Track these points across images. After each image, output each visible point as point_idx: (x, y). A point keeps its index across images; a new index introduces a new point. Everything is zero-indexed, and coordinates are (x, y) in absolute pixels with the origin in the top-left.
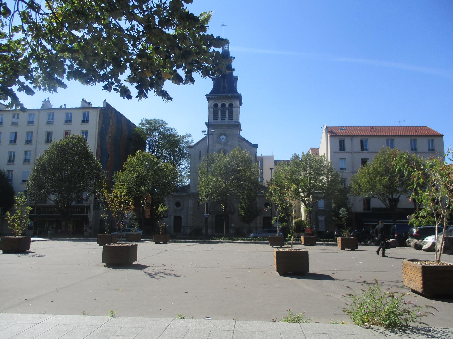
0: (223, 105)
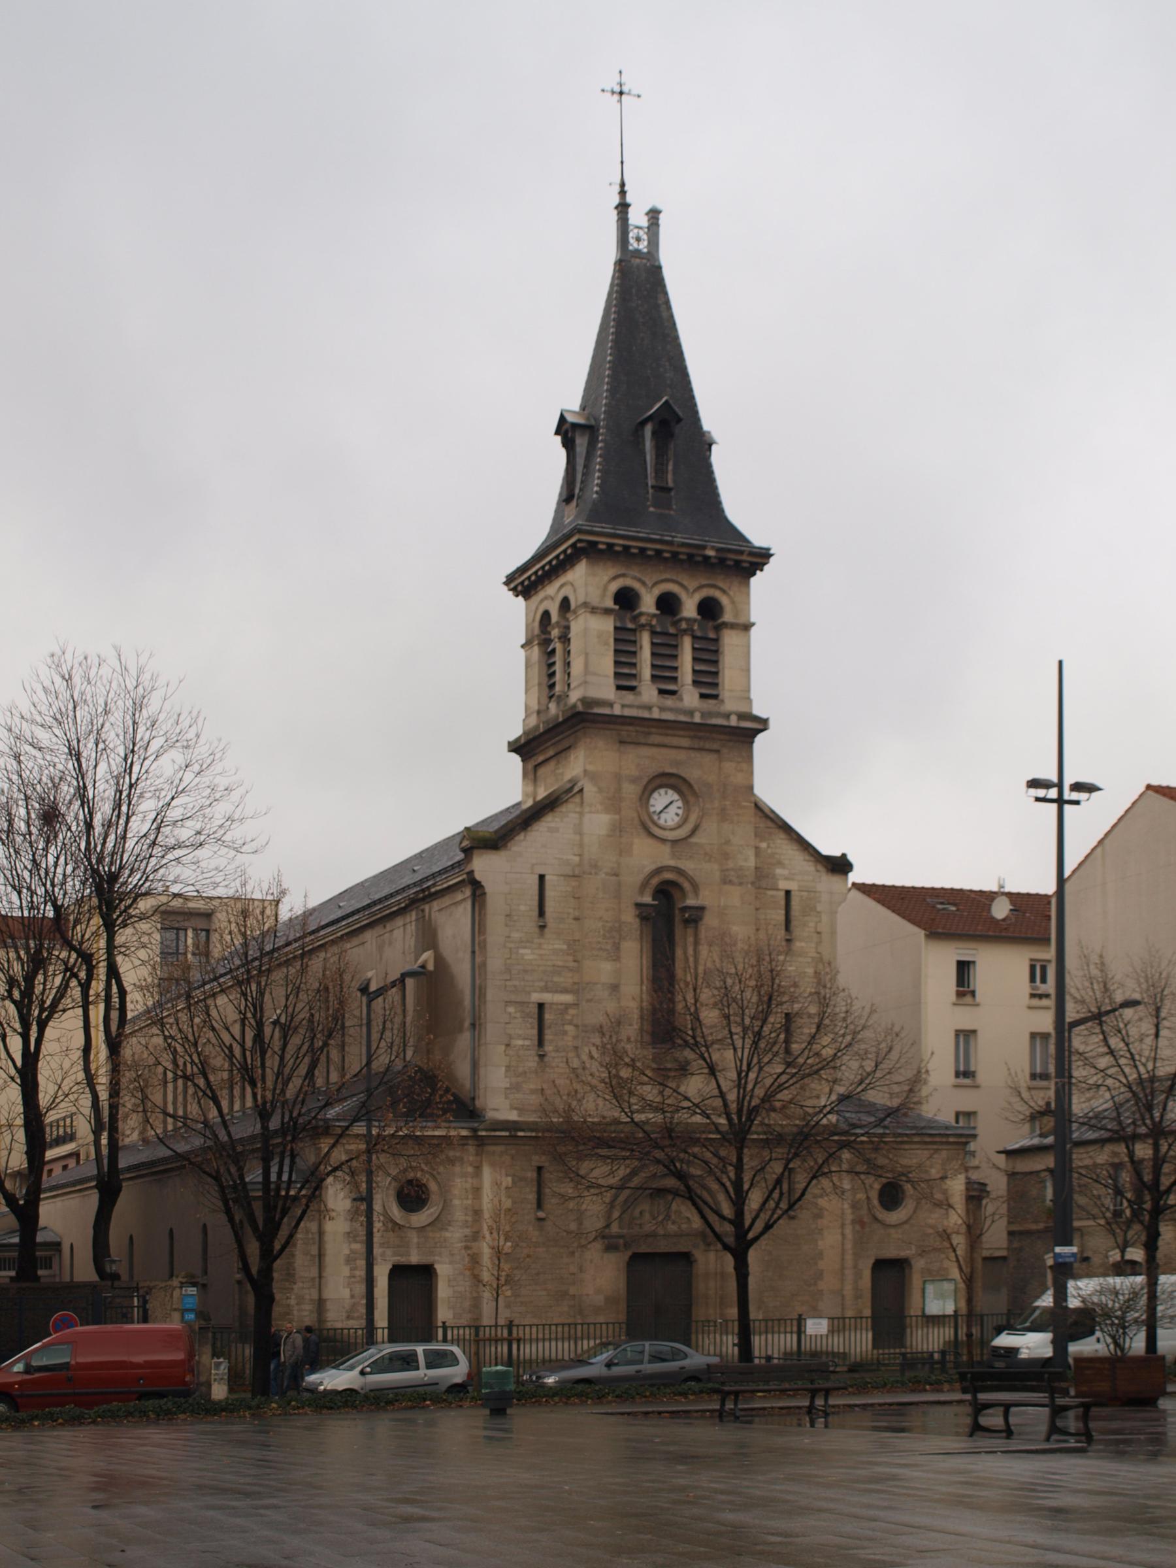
0: (668, 604)
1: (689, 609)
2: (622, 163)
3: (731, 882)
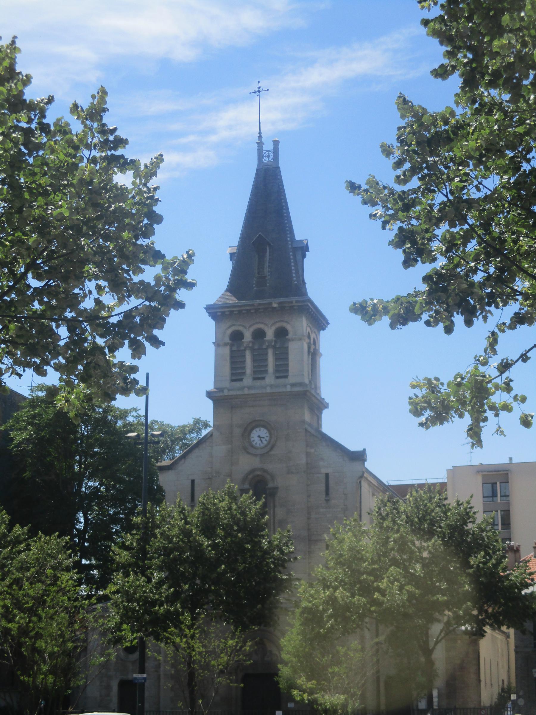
0: (259, 335)
1: (270, 335)
2: (260, 123)
3: (292, 473)
